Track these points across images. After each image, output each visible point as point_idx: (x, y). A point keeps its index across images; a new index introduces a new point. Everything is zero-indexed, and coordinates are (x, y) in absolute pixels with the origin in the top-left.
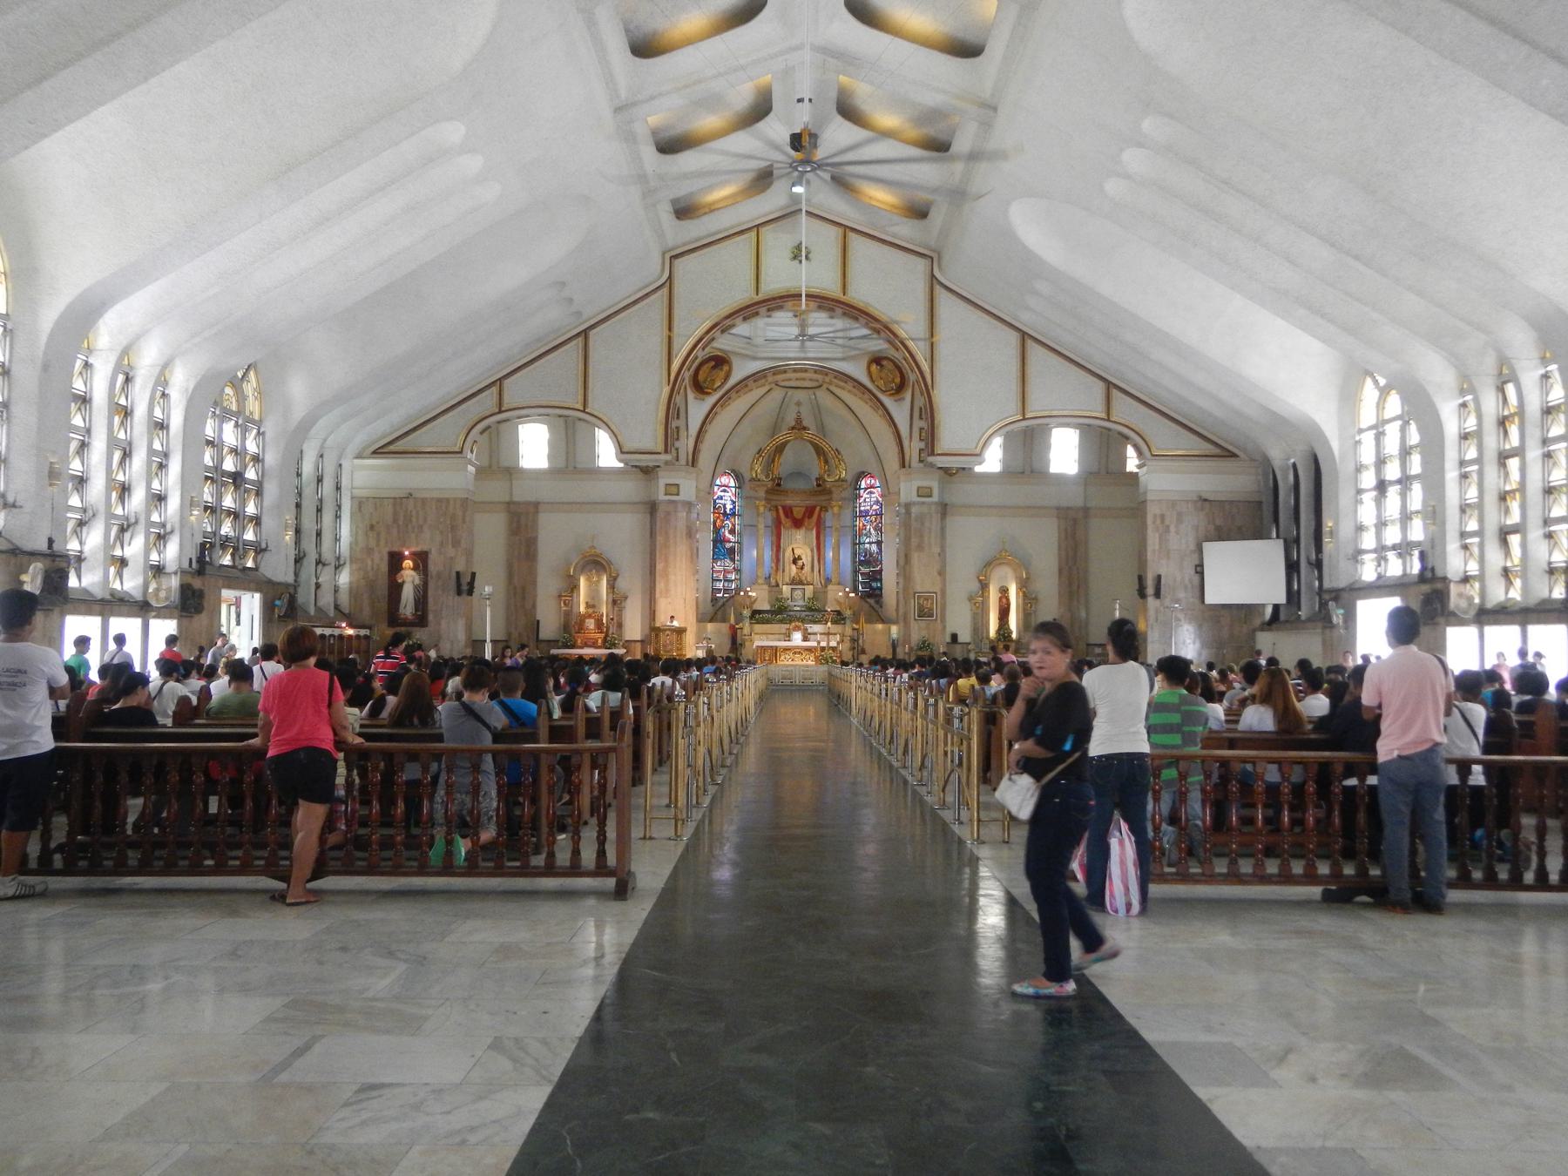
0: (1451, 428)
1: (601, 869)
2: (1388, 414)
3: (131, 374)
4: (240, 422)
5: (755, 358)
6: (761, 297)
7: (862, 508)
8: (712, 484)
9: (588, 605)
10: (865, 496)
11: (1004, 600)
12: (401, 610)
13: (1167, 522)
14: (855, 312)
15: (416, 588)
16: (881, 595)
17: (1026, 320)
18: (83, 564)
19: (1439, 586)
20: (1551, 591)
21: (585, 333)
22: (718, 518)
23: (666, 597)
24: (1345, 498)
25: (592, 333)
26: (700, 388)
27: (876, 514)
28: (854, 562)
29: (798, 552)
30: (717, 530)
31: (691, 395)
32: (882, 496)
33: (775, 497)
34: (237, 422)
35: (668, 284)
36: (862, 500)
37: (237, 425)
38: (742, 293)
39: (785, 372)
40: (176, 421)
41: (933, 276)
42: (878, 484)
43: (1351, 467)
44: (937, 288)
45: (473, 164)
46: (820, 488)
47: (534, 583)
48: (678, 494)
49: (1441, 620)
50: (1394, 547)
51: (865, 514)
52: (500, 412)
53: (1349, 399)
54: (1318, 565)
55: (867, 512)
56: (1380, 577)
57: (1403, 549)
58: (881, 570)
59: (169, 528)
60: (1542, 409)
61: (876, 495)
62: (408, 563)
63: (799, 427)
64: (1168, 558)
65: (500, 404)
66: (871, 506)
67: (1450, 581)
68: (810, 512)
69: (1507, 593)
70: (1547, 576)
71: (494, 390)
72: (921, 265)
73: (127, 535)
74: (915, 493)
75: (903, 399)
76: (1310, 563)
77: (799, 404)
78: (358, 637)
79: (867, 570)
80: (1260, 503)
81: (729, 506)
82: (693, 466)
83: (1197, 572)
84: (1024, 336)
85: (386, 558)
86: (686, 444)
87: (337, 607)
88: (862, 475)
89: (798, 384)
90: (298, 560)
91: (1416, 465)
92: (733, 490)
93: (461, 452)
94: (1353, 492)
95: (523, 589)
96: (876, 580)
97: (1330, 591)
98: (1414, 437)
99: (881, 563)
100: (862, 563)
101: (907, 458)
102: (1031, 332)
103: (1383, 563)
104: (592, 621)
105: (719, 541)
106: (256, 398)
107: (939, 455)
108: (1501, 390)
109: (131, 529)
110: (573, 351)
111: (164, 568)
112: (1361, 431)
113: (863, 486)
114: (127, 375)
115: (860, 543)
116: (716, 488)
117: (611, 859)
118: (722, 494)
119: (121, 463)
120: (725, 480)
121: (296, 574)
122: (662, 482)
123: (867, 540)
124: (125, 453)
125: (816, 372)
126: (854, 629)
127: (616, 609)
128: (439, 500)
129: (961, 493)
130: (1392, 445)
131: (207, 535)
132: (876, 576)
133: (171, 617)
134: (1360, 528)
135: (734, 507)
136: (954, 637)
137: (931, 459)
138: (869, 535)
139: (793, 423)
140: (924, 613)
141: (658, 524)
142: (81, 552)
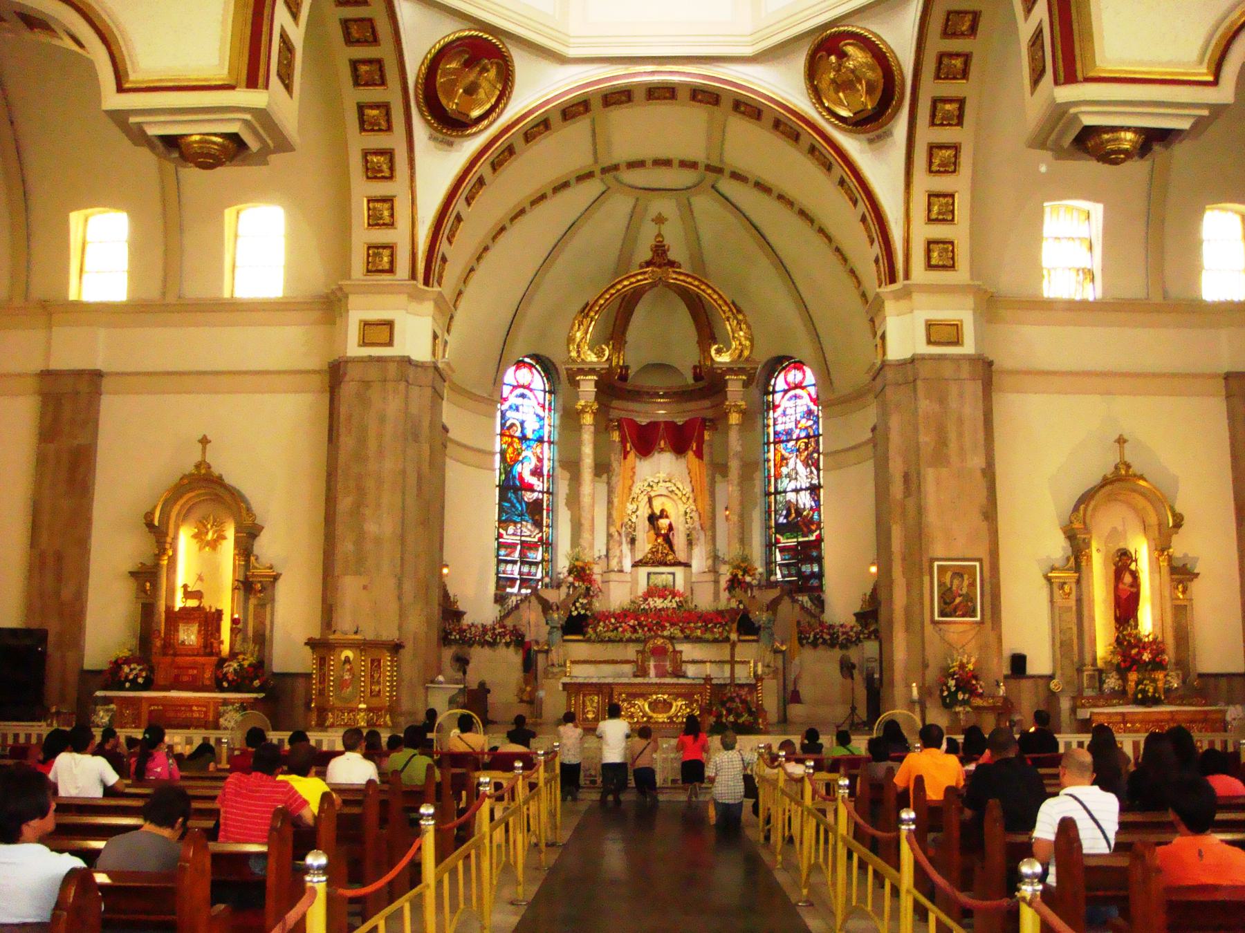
7: (779, 428)
8: (498, 382)
16: (820, 588)
22: (510, 444)
23: (357, 573)
27: (808, 437)
32: (815, 401)
36: (779, 411)
46: (701, 384)
47: (83, 544)
48: (390, 343)
55: (789, 433)
58: (820, 540)
61: (807, 400)
79: (792, 542)
82: (426, 282)
88: (779, 363)
92: (540, 395)
95: (59, 557)
96: (811, 560)
99: (819, 527)
100: (780, 529)
105: (510, 487)
115: (777, 492)
116: (506, 390)
118: (519, 401)
120: (524, 375)
122: (355, 317)
123: (792, 485)
127: (253, 602)
132: (810, 552)
135: (542, 427)
139: (648, 255)
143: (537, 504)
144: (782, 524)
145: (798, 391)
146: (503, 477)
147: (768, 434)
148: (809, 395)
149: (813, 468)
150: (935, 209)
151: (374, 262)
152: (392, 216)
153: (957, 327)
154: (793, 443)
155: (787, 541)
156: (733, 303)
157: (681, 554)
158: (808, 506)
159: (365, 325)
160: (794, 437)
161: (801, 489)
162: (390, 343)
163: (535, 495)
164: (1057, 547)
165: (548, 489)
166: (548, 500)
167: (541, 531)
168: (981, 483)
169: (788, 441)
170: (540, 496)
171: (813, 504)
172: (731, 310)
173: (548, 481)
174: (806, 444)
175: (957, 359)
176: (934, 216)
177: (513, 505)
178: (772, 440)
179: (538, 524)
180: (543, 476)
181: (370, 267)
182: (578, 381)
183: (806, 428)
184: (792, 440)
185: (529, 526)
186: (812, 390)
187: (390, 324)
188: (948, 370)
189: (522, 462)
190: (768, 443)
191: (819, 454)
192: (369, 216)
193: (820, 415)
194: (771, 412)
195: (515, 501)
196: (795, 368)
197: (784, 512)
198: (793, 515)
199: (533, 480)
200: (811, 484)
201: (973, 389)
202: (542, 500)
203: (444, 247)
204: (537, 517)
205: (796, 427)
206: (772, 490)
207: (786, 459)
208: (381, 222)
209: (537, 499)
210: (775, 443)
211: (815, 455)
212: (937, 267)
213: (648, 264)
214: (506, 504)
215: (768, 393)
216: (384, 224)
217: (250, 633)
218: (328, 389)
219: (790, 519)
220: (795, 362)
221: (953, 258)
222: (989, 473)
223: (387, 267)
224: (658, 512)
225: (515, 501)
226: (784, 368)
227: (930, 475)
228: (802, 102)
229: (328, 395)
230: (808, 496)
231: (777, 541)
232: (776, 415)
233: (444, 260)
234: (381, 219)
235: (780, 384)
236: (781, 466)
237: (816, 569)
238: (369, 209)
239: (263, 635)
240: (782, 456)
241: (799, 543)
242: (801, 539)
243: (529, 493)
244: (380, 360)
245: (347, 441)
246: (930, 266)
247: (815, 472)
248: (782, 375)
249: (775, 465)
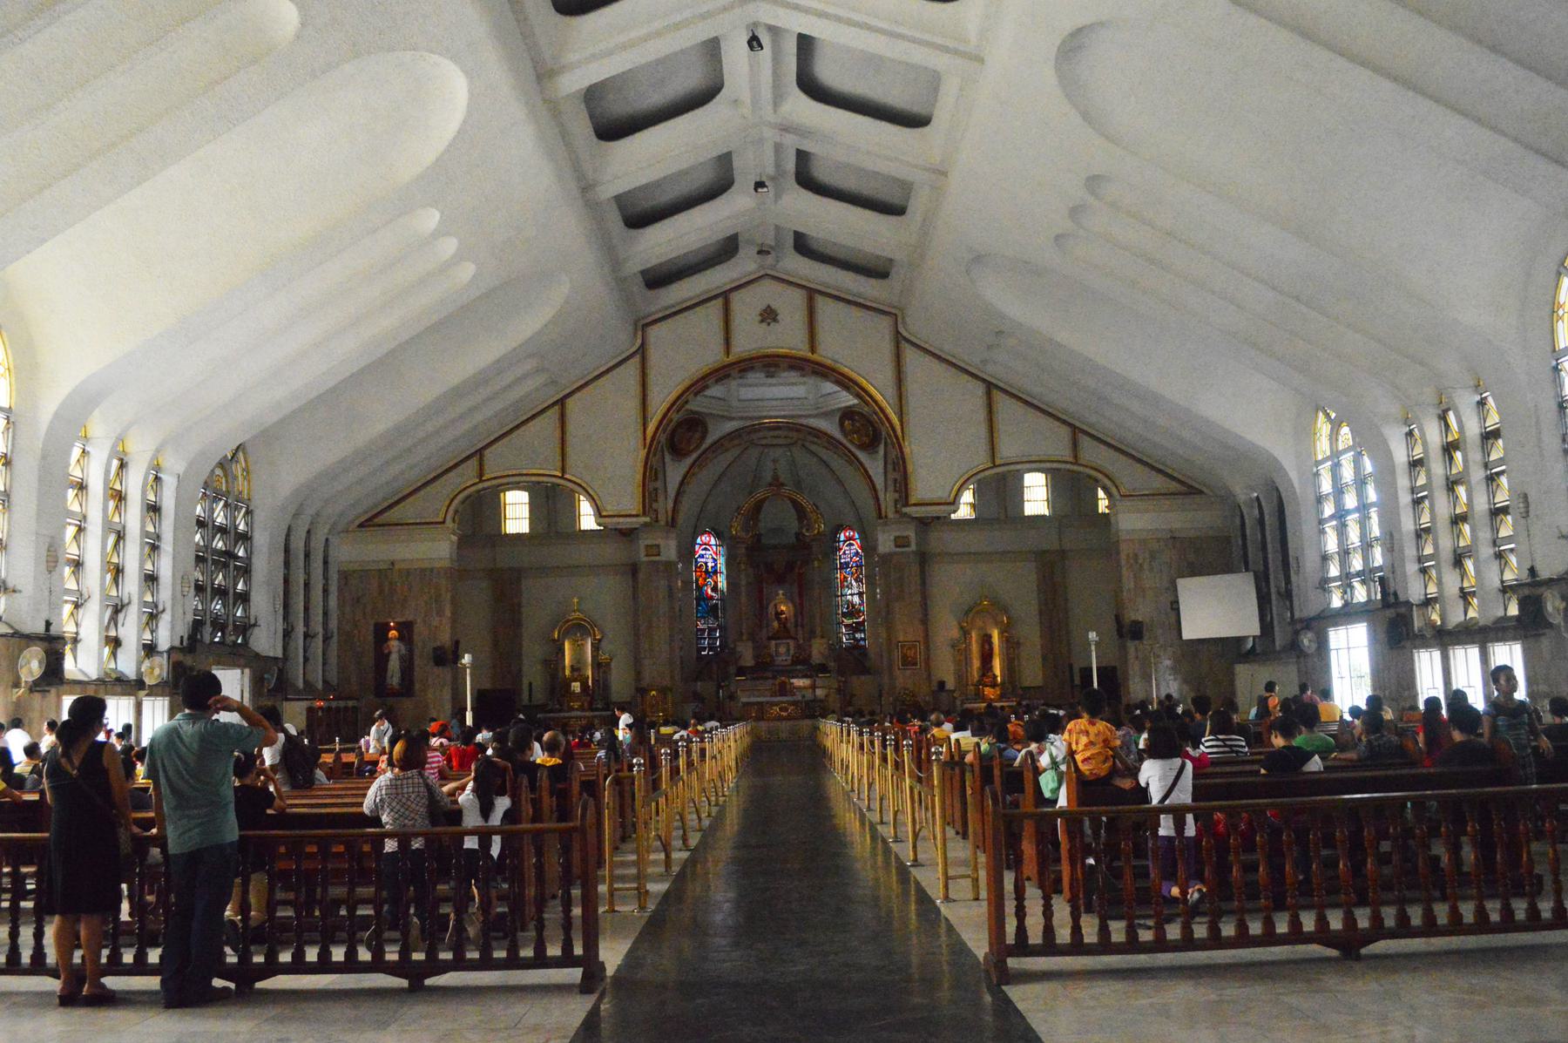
0: (1400, 456)
1: (567, 960)
2: (1341, 447)
3: (126, 459)
4: (230, 501)
5: (732, 419)
6: (732, 358)
9: (573, 669)
10: (845, 548)
11: (987, 647)
12: (388, 681)
13: (1140, 561)
14: (823, 371)
15: (401, 658)
17: (993, 371)
18: (79, 646)
19: (1403, 610)
20: (1506, 610)
21: (561, 402)
24: (1308, 529)
25: (570, 403)
26: (678, 451)
27: (857, 566)
31: (668, 458)
32: (861, 548)
34: (226, 502)
35: (641, 351)
37: (226, 505)
38: (713, 355)
39: (759, 430)
40: (168, 503)
41: (898, 332)
42: (857, 536)
43: (1312, 497)
44: (904, 345)
45: (449, 246)
49: (1408, 644)
50: (1358, 574)
51: (845, 566)
52: (481, 481)
53: (1306, 434)
54: (1288, 595)
55: (848, 563)
56: (1346, 604)
57: (1366, 575)
59: (161, 608)
60: (1482, 434)
62: (393, 633)
63: (777, 483)
64: (1144, 597)
65: (481, 474)
66: (851, 558)
67: (1413, 605)
68: (790, 567)
69: (1466, 614)
70: (1501, 595)
71: (474, 462)
72: (885, 324)
73: (121, 616)
74: (892, 544)
75: (877, 452)
76: (1279, 593)
77: (774, 461)
78: (346, 708)
80: (1228, 540)
81: (710, 565)
83: (1172, 609)
84: (990, 387)
85: (372, 628)
86: (665, 505)
87: (325, 682)
89: (775, 441)
90: (287, 634)
91: (1372, 495)
92: (714, 548)
93: (444, 522)
94: (1315, 523)
97: (1301, 620)
98: (1368, 466)
100: (844, 615)
101: (883, 510)
102: (993, 381)
103: (1349, 590)
104: (578, 684)
106: (245, 478)
107: (915, 505)
108: (1443, 418)
109: (124, 611)
110: (549, 420)
111: (156, 646)
112: (1318, 463)
113: (842, 538)
114: (121, 460)
115: (842, 595)
116: (697, 547)
117: (578, 950)
118: (704, 552)
119: (115, 546)
120: (705, 538)
121: (285, 648)
123: (849, 592)
124: (119, 536)
125: (791, 429)
126: (839, 682)
127: (601, 670)
128: (423, 570)
129: (939, 540)
130: (1348, 473)
131: (197, 613)
133: (162, 695)
134: (1325, 558)
135: (716, 565)
136: (942, 684)
137: (906, 510)
140: (908, 662)
142: (77, 633)
155: (847, 621)
157: (792, 631)
164: (955, 633)
186: (858, 541)
187: (658, 546)
215: (836, 542)
228: (837, 434)
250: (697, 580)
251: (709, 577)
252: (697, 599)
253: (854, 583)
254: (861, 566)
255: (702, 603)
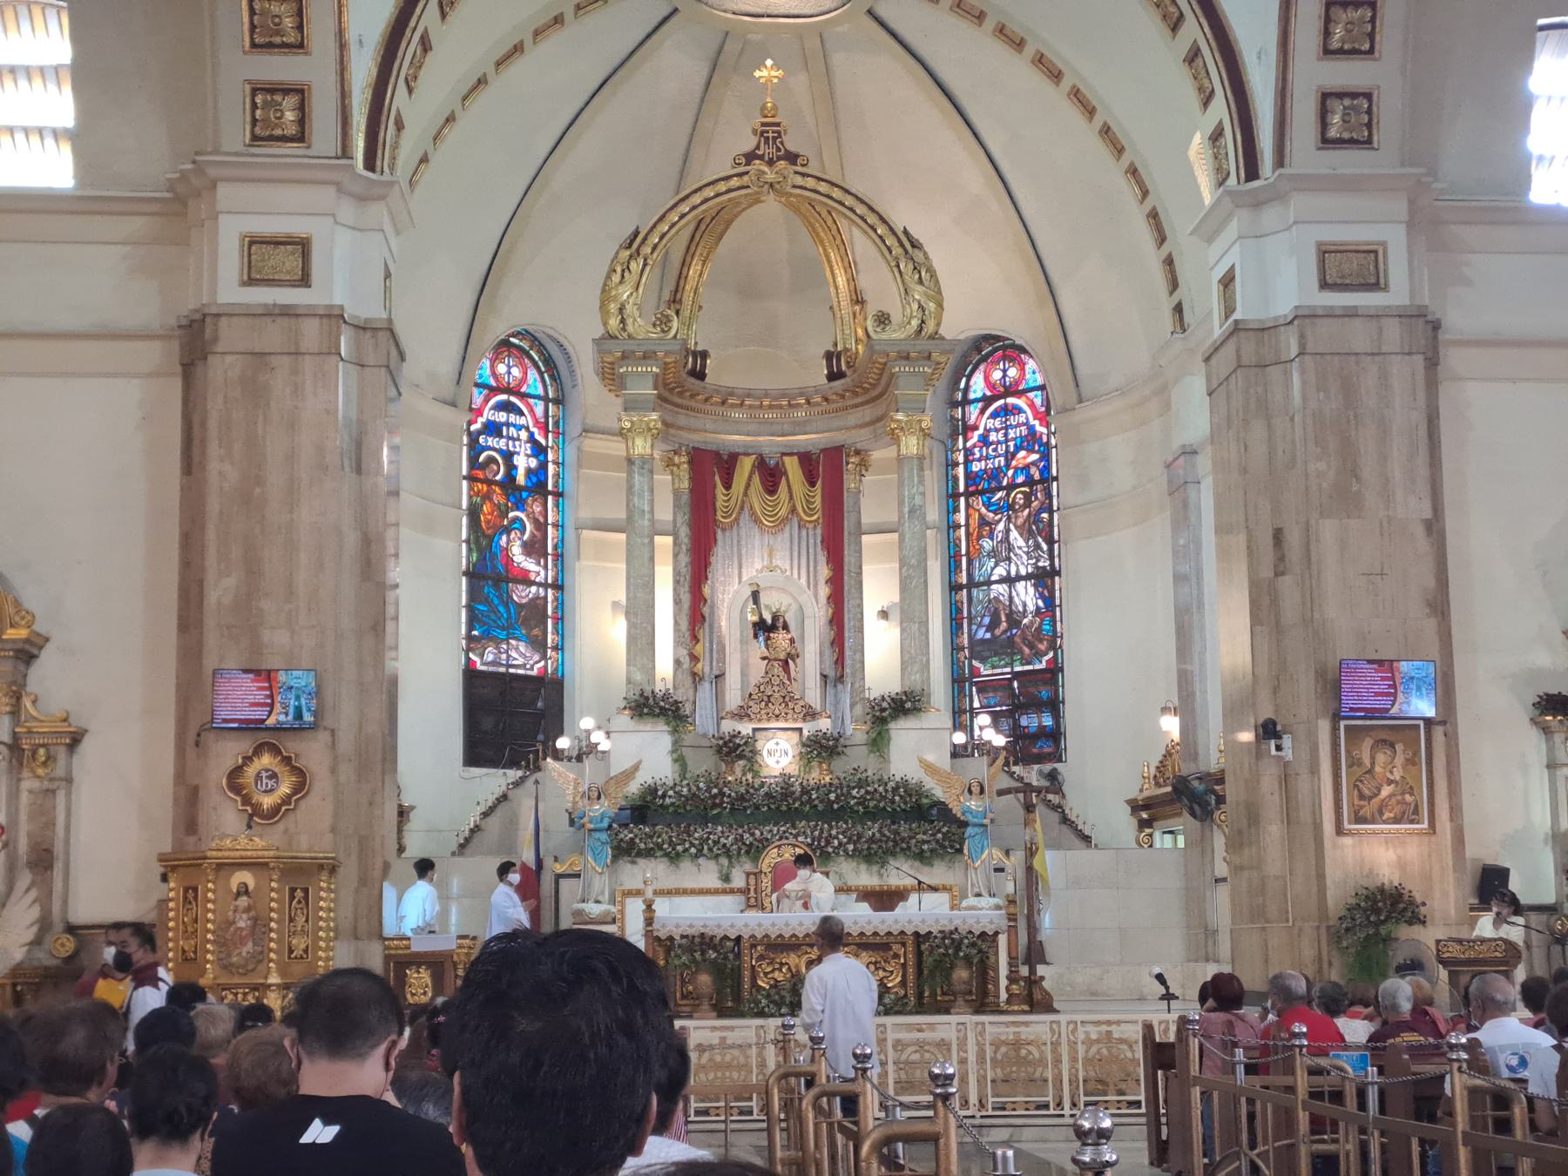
7: (976, 467)
22: (487, 497)
27: (1030, 482)
28: (955, 648)
29: (772, 601)
30: (482, 537)
33: (682, 420)
36: (975, 437)
46: (838, 384)
48: (305, 280)
55: (996, 474)
58: (1054, 672)
66: (1010, 456)
81: (523, 462)
82: (370, 164)
92: (539, 408)
96: (1037, 705)
99: (1053, 646)
100: (981, 650)
115: (972, 584)
118: (502, 417)
120: (509, 370)
122: (230, 232)
123: (1000, 571)
135: (543, 466)
138: (1004, 553)
141: (215, 406)
143: (537, 606)
144: (983, 641)
145: (1011, 400)
146: (475, 556)
147: (956, 479)
148: (1032, 405)
149: (1040, 540)
150: (1338, 32)
151: (266, 120)
152: (300, 27)
153: (1373, 254)
154: (1000, 494)
156: (906, 232)
158: (1031, 607)
159: (251, 243)
160: (1005, 483)
161: (1019, 578)
162: (305, 280)
163: (534, 589)
165: (556, 579)
166: (556, 599)
167: (544, 657)
168: (1423, 543)
169: (993, 491)
170: (541, 590)
171: (1040, 603)
172: (902, 245)
173: (555, 566)
174: (1027, 497)
175: (1376, 316)
176: (1335, 44)
177: (495, 611)
178: (962, 489)
179: (539, 645)
180: (545, 555)
181: (258, 130)
182: (622, 376)
183: (1027, 467)
184: (1000, 488)
185: (522, 649)
186: (1037, 397)
187: (303, 246)
188: (1359, 337)
189: (508, 531)
190: (955, 496)
191: (1051, 512)
192: (253, 27)
193: (1053, 442)
194: (961, 437)
195: (496, 601)
196: (1004, 358)
197: (987, 620)
198: (1004, 625)
199: (530, 565)
200: (1037, 568)
201: (1405, 372)
202: (546, 598)
203: (399, 99)
204: (536, 632)
205: (1008, 466)
206: (964, 579)
207: (989, 524)
208: (277, 40)
209: (537, 598)
210: (968, 494)
211: (1045, 515)
212: (1339, 142)
213: (750, 157)
214: (481, 607)
215: (954, 404)
216: (284, 45)
217: (23, 845)
218: (179, 369)
219: (998, 632)
220: (1004, 348)
221: (1369, 125)
222: (1435, 527)
223: (292, 130)
224: (768, 618)
225: (496, 601)
226: (984, 359)
227: (1328, 530)
229: (178, 383)
230: (1031, 590)
231: (975, 672)
232: (969, 444)
233: (400, 126)
234: (278, 33)
235: (978, 387)
236: (980, 537)
237: (1048, 721)
238: (252, 12)
239: (49, 851)
240: (981, 517)
241: (1016, 675)
242: (1018, 669)
243: (520, 587)
244: (288, 312)
245: (221, 470)
246: (1326, 142)
247: (1045, 547)
248: (982, 367)
249: (968, 534)
250: (474, 513)
251: (520, 505)
252: (475, 575)
253: (1016, 538)
254: (1047, 479)
255: (488, 590)
